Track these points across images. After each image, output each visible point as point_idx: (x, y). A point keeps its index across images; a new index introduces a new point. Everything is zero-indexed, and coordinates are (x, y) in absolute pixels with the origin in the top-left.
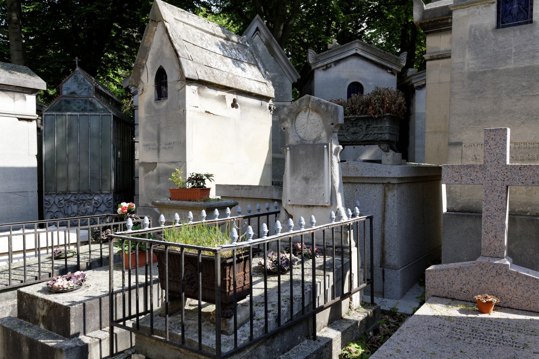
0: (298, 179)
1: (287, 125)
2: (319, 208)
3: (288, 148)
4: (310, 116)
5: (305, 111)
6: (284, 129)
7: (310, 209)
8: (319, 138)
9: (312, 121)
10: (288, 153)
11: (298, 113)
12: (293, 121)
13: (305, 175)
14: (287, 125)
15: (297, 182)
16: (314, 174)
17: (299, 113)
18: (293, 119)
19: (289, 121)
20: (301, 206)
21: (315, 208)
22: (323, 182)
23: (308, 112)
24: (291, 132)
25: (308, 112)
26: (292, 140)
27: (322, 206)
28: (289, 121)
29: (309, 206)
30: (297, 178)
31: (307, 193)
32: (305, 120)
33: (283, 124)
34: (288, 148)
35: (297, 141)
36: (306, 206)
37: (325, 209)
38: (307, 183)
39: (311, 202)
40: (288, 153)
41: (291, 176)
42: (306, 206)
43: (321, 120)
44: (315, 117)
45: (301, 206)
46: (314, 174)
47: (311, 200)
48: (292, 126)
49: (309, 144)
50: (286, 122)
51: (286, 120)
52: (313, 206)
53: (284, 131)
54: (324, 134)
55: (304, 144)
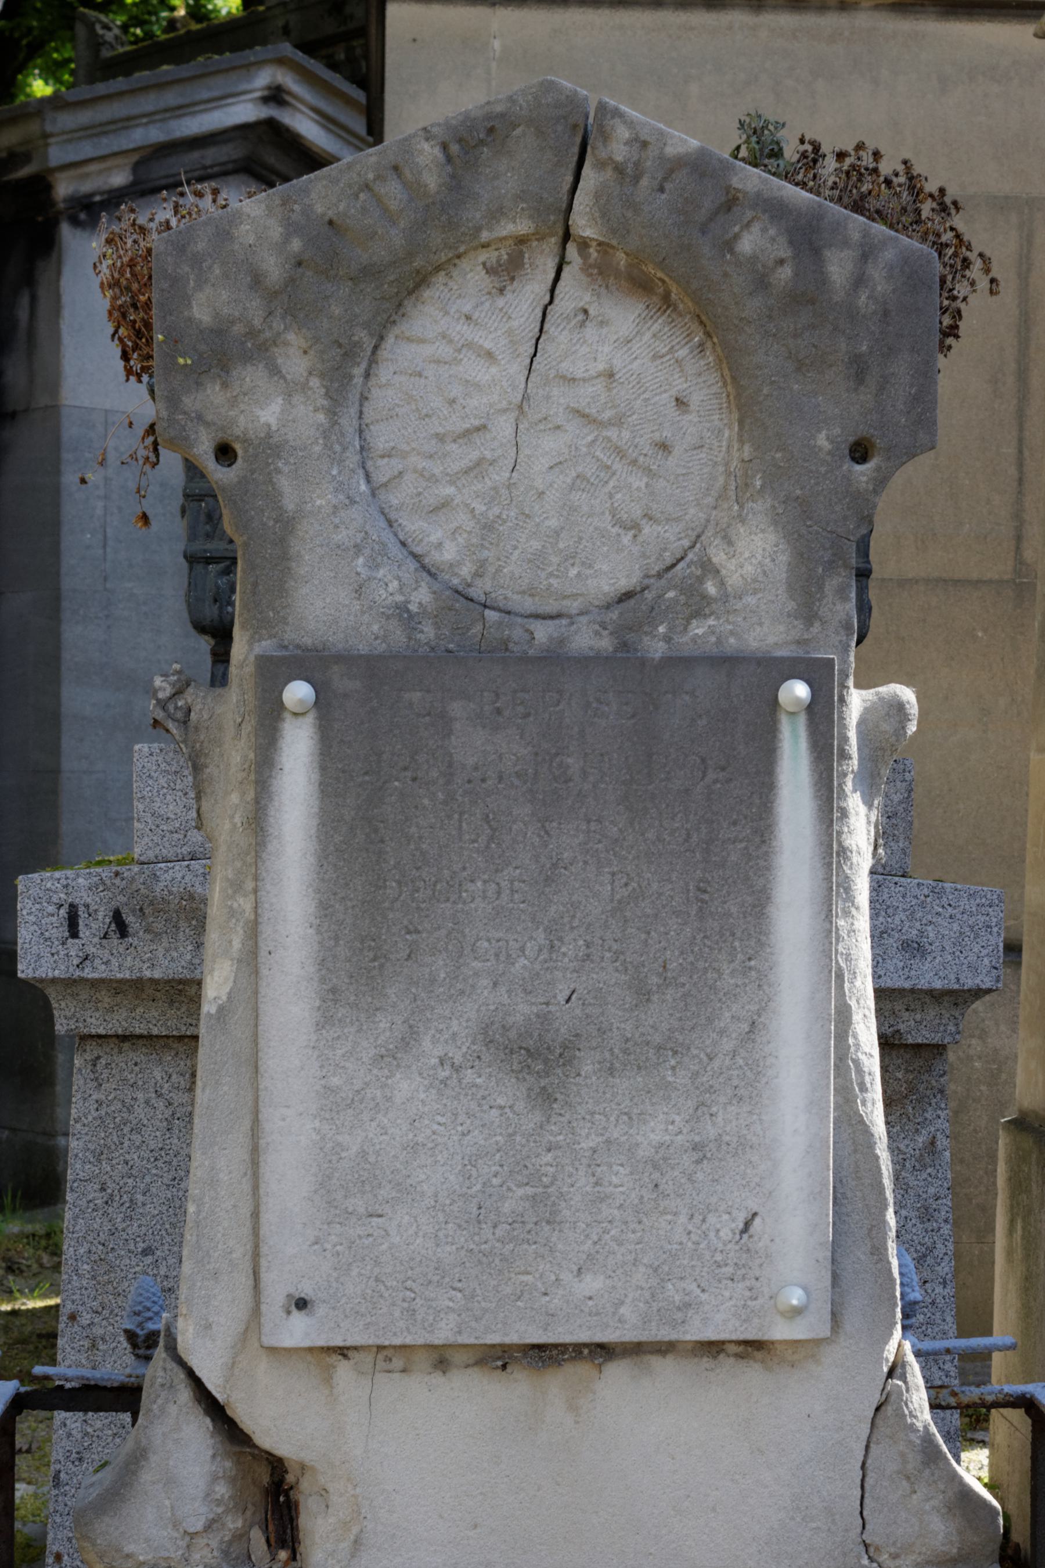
0: (431, 1049)
1: (272, 406)
2: (664, 1366)
3: (298, 692)
4: (559, 335)
5: (508, 270)
6: (225, 453)
7: (556, 1383)
8: (683, 583)
9: (586, 396)
10: (298, 747)
11: (404, 282)
12: (348, 366)
13: (523, 1010)
14: (269, 414)
15: (405, 1086)
16: (643, 995)
17: (421, 281)
18: (349, 353)
19: (295, 359)
20: (441, 1359)
21: (617, 1371)
22: (750, 1083)
23: (532, 289)
24: (323, 499)
25: (532, 289)
26: (331, 591)
27: (713, 1348)
28: (295, 359)
29: (544, 1355)
30: (408, 1040)
31: (546, 1209)
32: (501, 377)
33: (212, 396)
34: (298, 692)
35: (402, 613)
36: (500, 1358)
37: (752, 1375)
38: (545, 1098)
39: (582, 1301)
40: (298, 747)
41: (325, 1020)
42: (500, 1358)
43: (704, 388)
44: (624, 355)
45: (441, 1359)
46: (643, 995)
47: (592, 1284)
48: (331, 430)
49: (555, 659)
50: (251, 376)
51: (259, 349)
52: (603, 1352)
53: (219, 474)
54: (753, 555)
55: (498, 652)
